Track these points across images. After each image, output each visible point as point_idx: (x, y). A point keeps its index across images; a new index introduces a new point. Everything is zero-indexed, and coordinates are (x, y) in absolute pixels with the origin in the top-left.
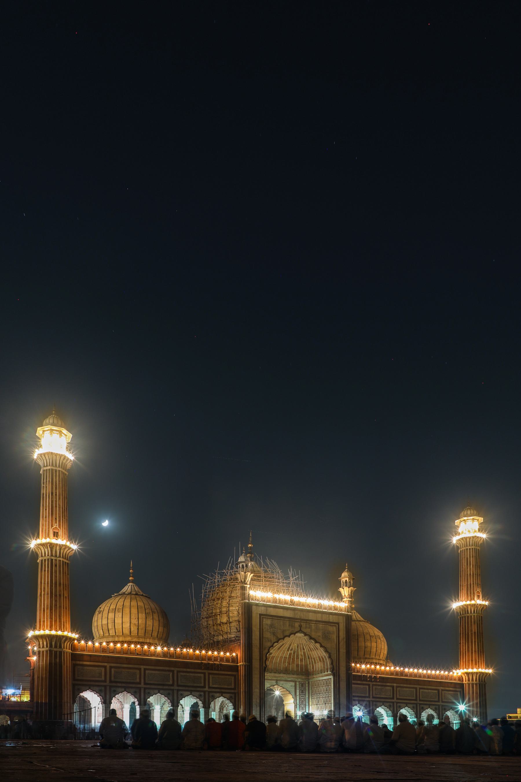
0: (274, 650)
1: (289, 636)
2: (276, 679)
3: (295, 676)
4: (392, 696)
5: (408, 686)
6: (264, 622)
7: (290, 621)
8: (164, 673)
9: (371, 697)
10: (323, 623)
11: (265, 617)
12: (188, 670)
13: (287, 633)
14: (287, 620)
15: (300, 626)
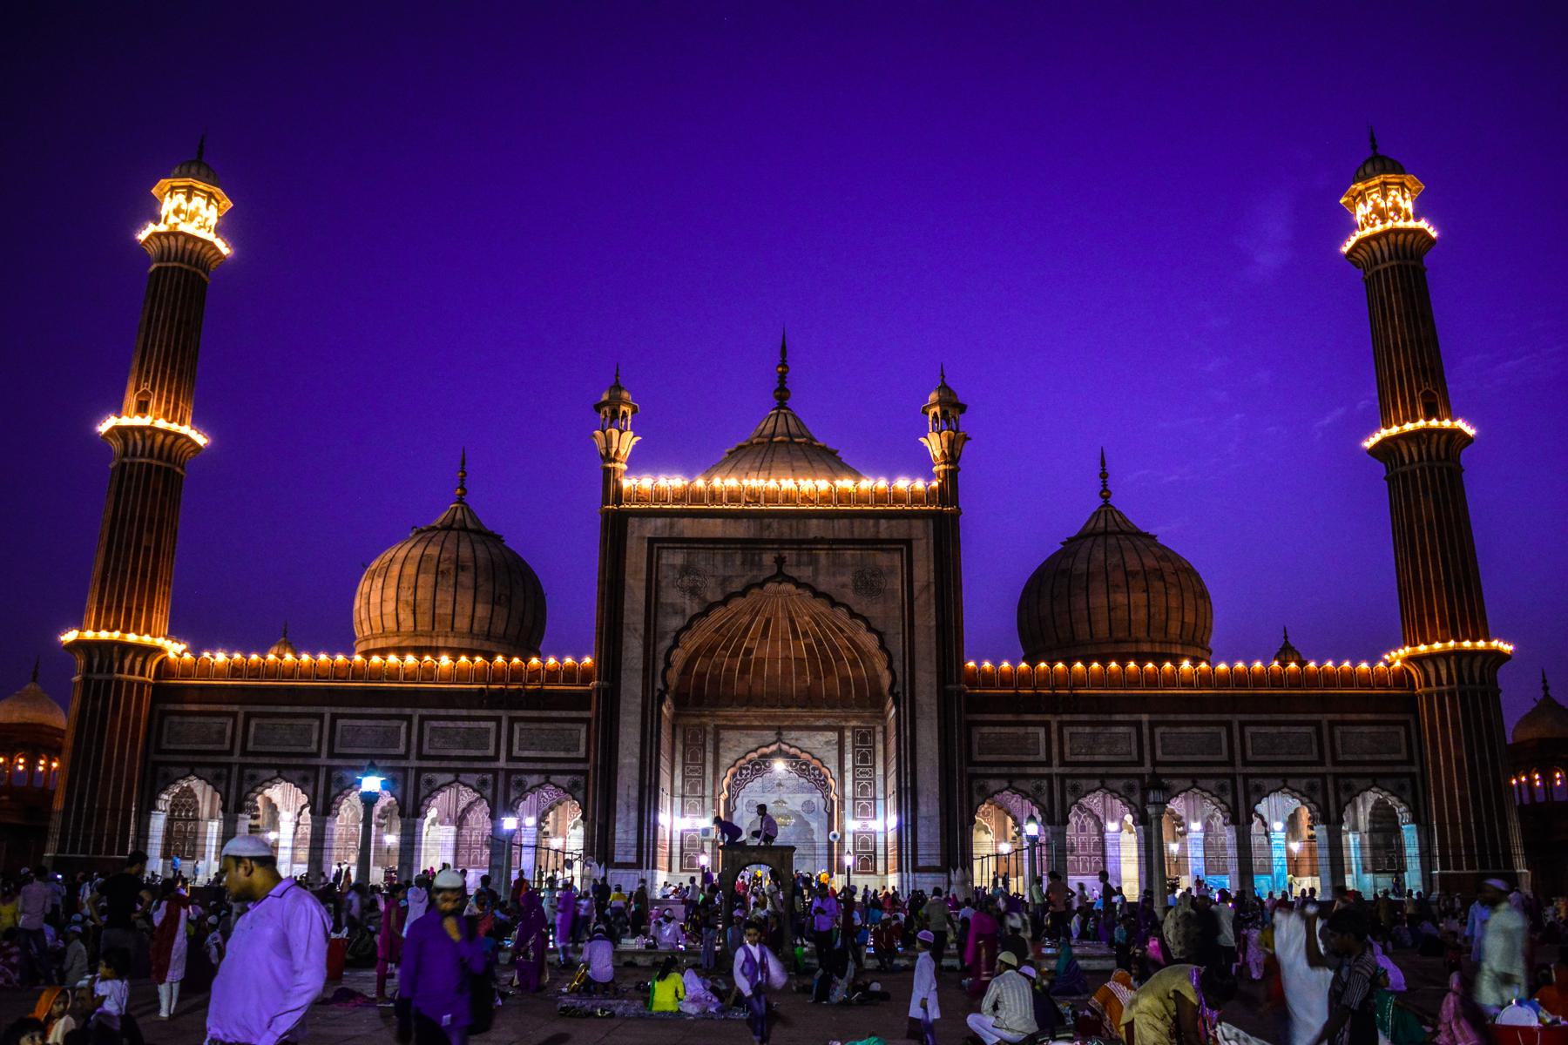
0: (752, 639)
1: (743, 594)
2: (777, 724)
3: (838, 711)
4: (1135, 757)
5: (1197, 717)
6: (664, 561)
7: (746, 549)
8: (384, 723)
9: (1056, 761)
10: (853, 544)
11: (666, 545)
12: (452, 712)
13: (737, 586)
14: (736, 549)
15: (780, 561)
